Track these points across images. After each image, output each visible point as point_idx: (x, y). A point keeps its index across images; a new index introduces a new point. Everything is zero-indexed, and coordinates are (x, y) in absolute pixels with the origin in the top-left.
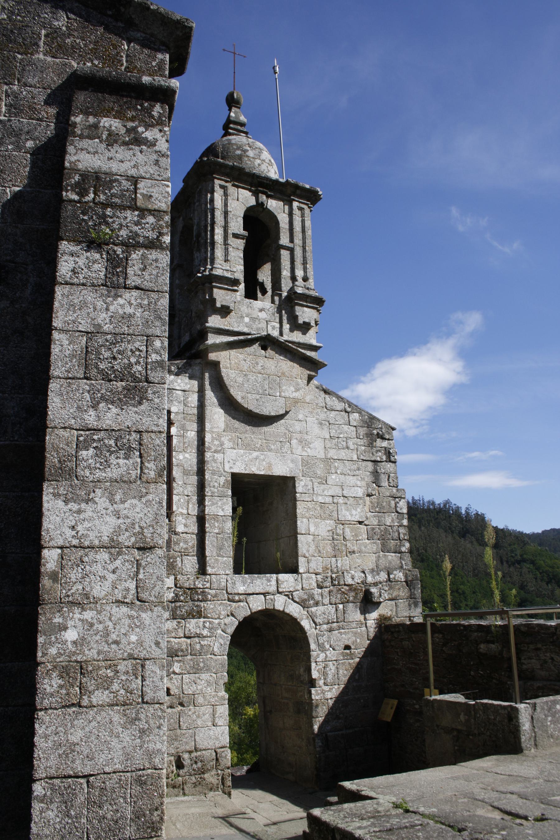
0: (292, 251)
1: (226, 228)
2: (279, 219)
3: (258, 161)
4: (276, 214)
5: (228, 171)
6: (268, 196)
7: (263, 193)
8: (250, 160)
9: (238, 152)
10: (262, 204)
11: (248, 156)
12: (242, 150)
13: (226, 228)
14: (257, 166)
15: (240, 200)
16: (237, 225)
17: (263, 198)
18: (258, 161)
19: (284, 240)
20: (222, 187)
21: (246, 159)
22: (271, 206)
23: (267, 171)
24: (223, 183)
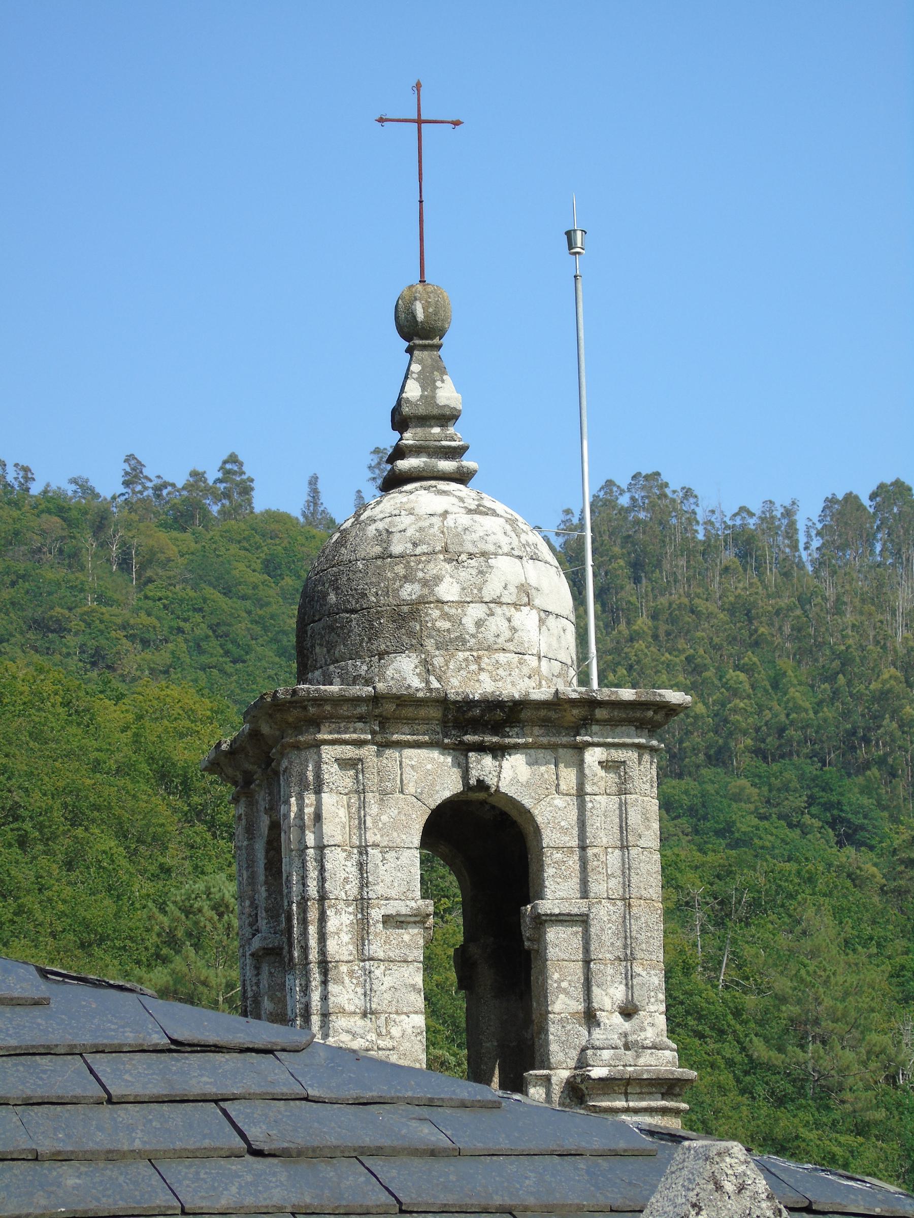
0: (583, 920)
1: (362, 903)
2: (539, 820)
3: (475, 612)
4: (527, 802)
5: (363, 709)
6: (499, 751)
7: (481, 748)
8: (445, 616)
9: (410, 591)
10: (482, 785)
11: (439, 601)
12: (425, 583)
13: (362, 903)
14: (472, 630)
15: (411, 789)
16: (400, 875)
17: (484, 766)
18: (475, 612)
19: (557, 892)
20: (345, 764)
21: (436, 613)
22: (515, 780)
23: (507, 634)
24: (349, 752)
